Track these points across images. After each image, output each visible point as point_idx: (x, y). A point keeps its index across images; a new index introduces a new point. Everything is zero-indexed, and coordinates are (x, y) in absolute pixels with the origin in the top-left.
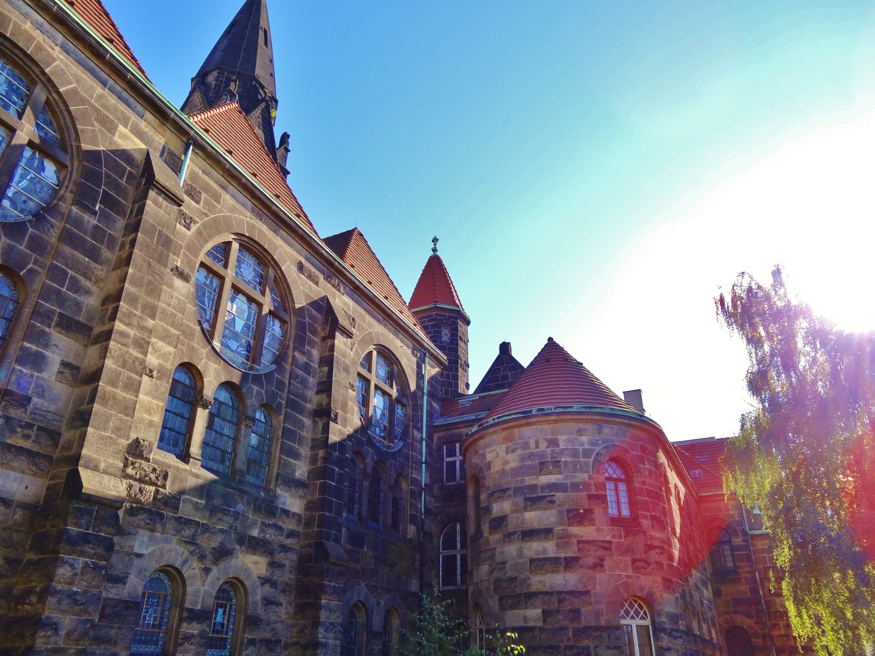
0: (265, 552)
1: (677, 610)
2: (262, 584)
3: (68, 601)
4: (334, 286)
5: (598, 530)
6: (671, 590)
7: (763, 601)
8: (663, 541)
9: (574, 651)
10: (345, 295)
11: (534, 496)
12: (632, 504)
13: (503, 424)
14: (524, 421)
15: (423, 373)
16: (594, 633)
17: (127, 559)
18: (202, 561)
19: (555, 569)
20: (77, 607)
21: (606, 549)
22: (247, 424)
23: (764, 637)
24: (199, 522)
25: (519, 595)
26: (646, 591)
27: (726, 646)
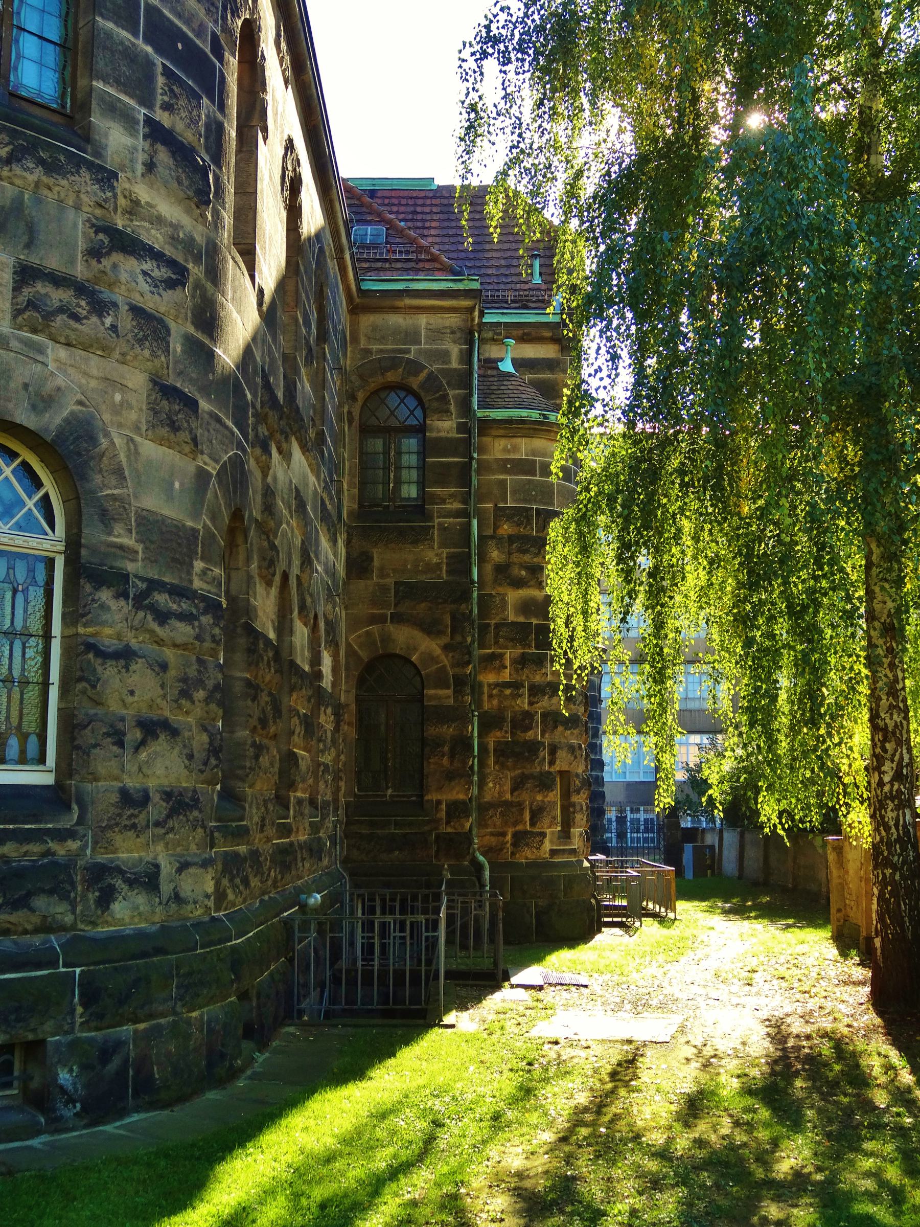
1: (196, 515)
6: (184, 436)
7: (475, 595)
23: (460, 683)
26: (65, 413)
27: (353, 707)
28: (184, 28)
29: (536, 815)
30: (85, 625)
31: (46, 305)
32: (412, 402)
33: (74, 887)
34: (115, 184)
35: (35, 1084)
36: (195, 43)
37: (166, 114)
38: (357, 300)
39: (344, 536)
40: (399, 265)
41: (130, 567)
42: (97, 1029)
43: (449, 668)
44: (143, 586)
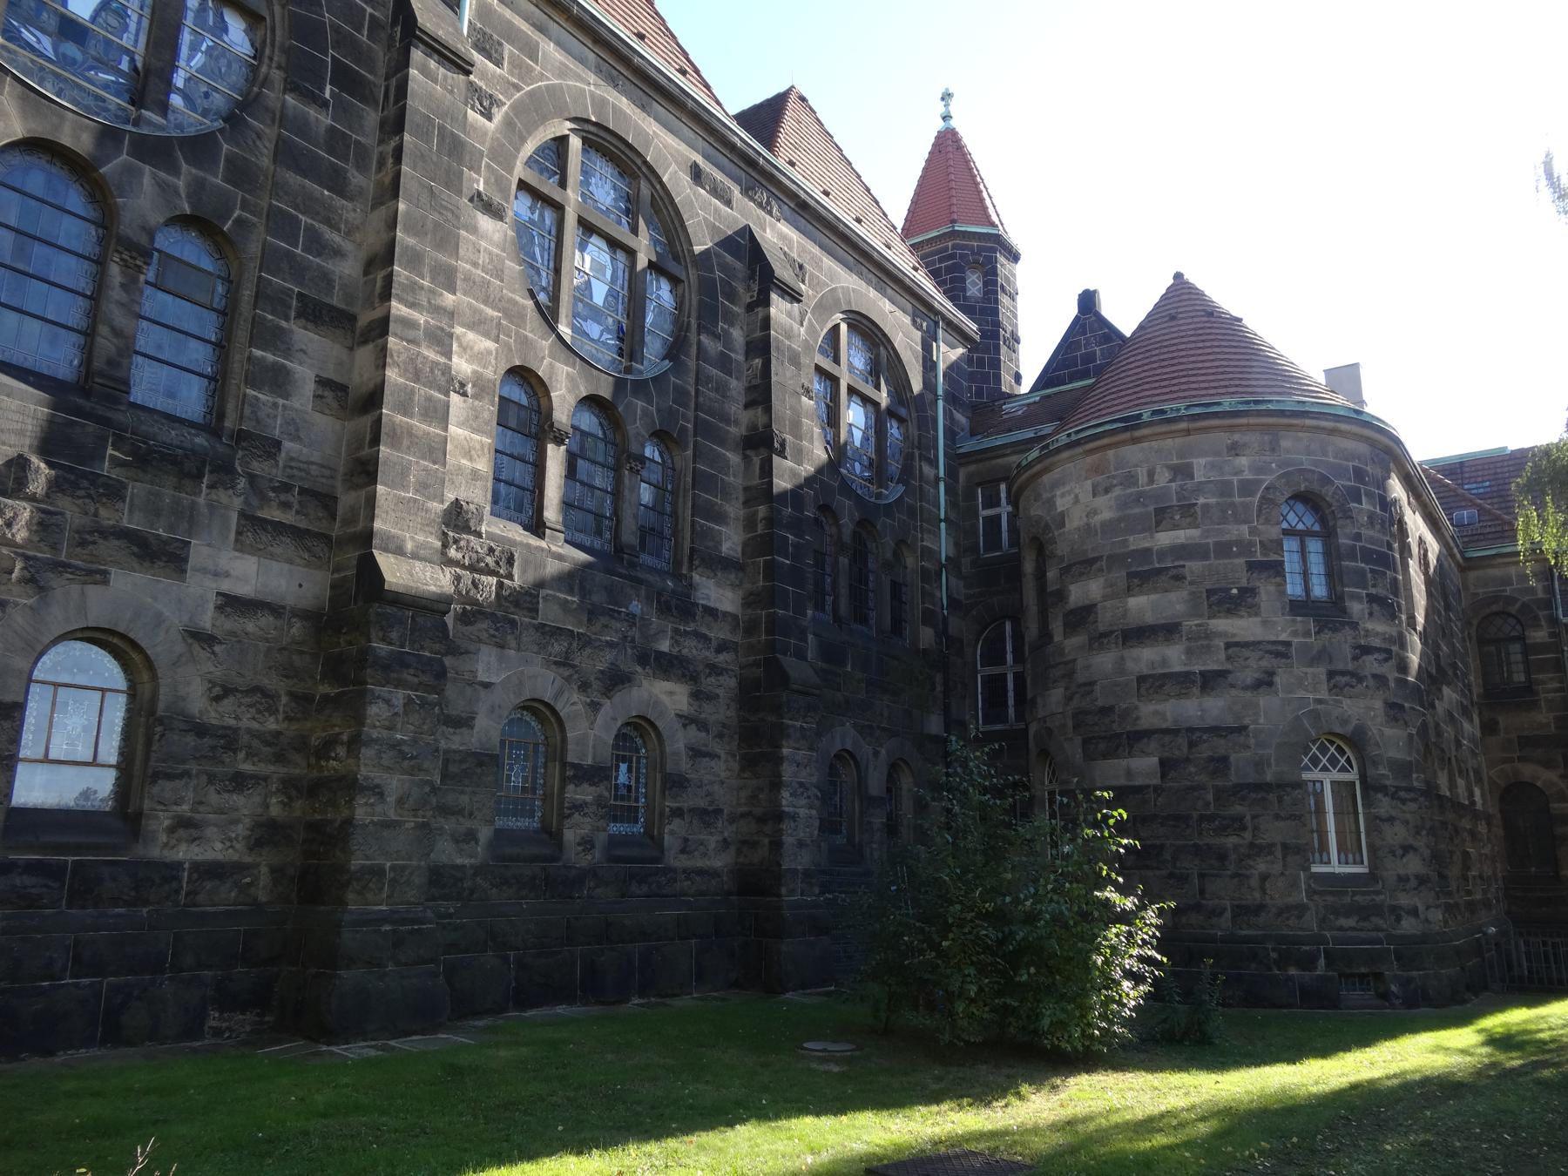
0: (684, 676)
2: (685, 726)
3: (392, 753)
4: (760, 205)
5: (1265, 623)
6: (1402, 722)
8: (1391, 640)
9: (1217, 823)
10: (782, 221)
11: (1146, 568)
12: (1332, 575)
13: (1086, 443)
14: (1127, 435)
15: (935, 358)
16: (1253, 795)
17: (469, 690)
18: (584, 691)
19: (1183, 691)
20: (406, 763)
21: (1278, 655)
22: (631, 468)
24: (572, 631)
25: (1119, 735)
27: (1499, 816)
32: (1512, 621)
39: (1477, 711)
40: (1490, 536)
41: (1388, 783)
44: (1393, 789)
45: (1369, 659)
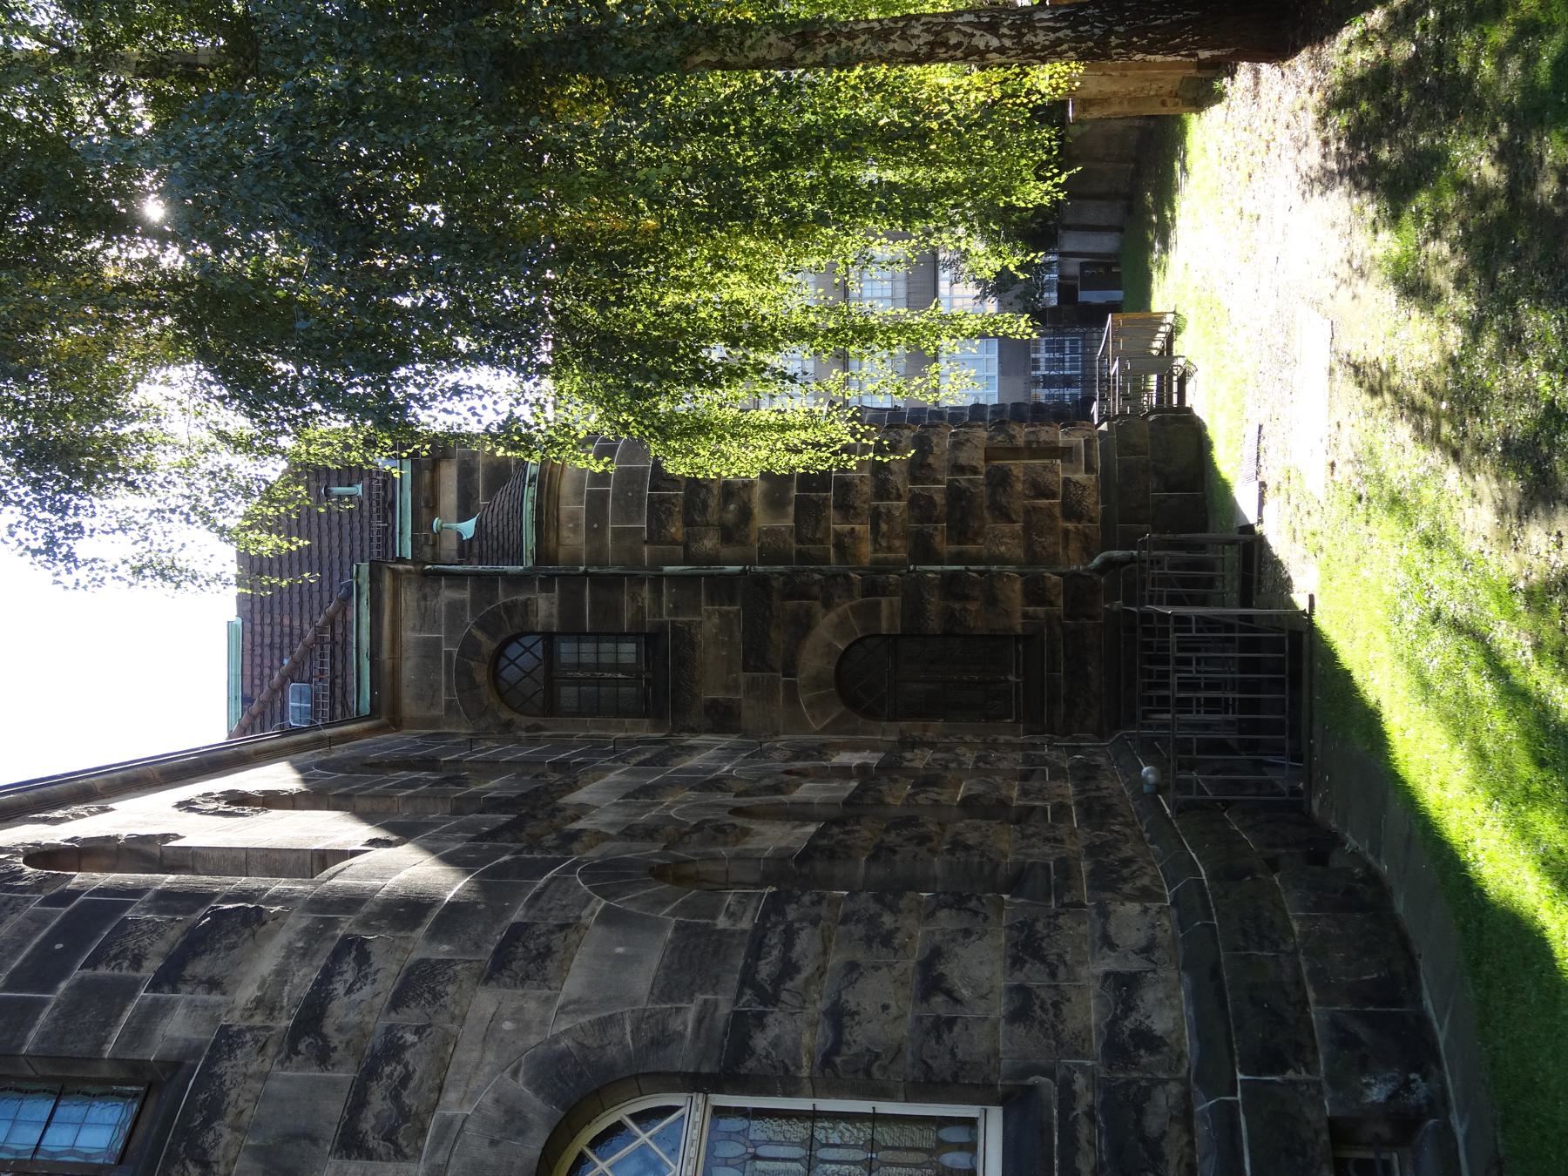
1: (659, 926)
6: (557, 941)
7: (760, 569)
26: (528, 1092)
27: (903, 724)
28: (36, 940)
29: (1041, 491)
30: (799, 1067)
31: (390, 1117)
32: (514, 650)
33: (1135, 1081)
34: (235, 1029)
35: (1385, 1131)
36: (56, 927)
37: (146, 964)
38: (384, 720)
39: (685, 736)
40: (339, 666)
41: (725, 1009)
42: (1315, 1050)
43: (853, 603)
44: (748, 994)
45: (340, 1012)
